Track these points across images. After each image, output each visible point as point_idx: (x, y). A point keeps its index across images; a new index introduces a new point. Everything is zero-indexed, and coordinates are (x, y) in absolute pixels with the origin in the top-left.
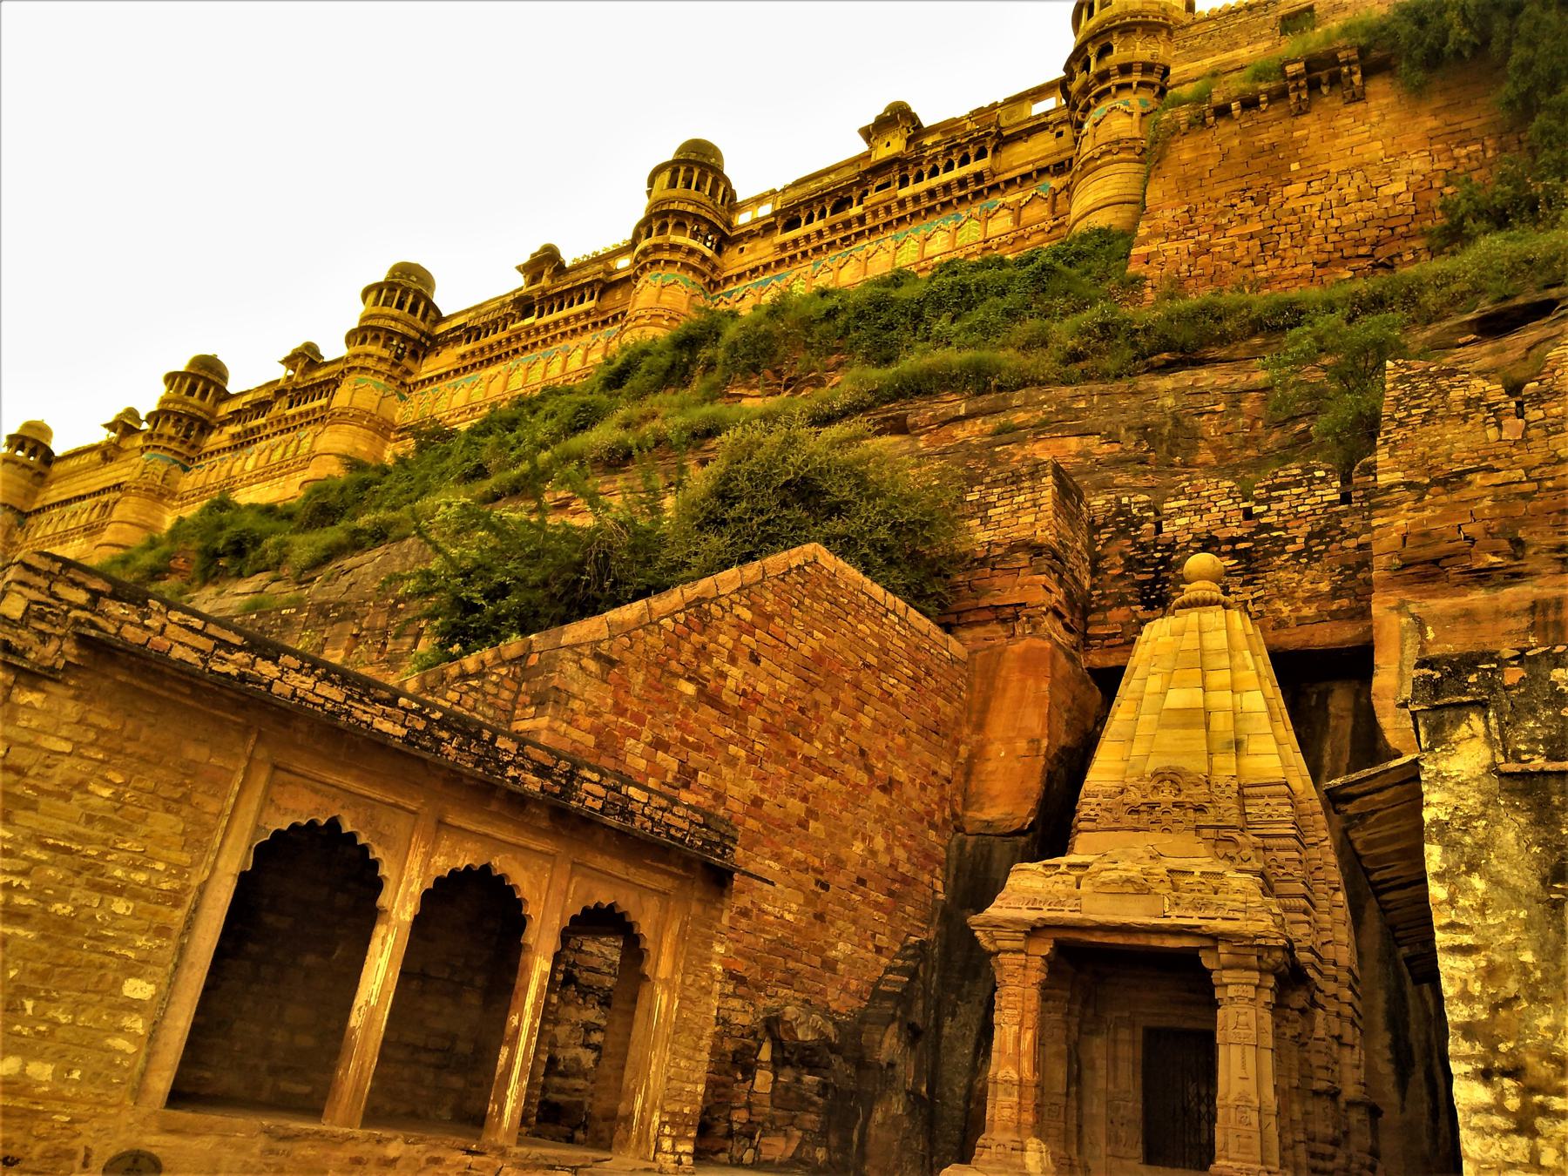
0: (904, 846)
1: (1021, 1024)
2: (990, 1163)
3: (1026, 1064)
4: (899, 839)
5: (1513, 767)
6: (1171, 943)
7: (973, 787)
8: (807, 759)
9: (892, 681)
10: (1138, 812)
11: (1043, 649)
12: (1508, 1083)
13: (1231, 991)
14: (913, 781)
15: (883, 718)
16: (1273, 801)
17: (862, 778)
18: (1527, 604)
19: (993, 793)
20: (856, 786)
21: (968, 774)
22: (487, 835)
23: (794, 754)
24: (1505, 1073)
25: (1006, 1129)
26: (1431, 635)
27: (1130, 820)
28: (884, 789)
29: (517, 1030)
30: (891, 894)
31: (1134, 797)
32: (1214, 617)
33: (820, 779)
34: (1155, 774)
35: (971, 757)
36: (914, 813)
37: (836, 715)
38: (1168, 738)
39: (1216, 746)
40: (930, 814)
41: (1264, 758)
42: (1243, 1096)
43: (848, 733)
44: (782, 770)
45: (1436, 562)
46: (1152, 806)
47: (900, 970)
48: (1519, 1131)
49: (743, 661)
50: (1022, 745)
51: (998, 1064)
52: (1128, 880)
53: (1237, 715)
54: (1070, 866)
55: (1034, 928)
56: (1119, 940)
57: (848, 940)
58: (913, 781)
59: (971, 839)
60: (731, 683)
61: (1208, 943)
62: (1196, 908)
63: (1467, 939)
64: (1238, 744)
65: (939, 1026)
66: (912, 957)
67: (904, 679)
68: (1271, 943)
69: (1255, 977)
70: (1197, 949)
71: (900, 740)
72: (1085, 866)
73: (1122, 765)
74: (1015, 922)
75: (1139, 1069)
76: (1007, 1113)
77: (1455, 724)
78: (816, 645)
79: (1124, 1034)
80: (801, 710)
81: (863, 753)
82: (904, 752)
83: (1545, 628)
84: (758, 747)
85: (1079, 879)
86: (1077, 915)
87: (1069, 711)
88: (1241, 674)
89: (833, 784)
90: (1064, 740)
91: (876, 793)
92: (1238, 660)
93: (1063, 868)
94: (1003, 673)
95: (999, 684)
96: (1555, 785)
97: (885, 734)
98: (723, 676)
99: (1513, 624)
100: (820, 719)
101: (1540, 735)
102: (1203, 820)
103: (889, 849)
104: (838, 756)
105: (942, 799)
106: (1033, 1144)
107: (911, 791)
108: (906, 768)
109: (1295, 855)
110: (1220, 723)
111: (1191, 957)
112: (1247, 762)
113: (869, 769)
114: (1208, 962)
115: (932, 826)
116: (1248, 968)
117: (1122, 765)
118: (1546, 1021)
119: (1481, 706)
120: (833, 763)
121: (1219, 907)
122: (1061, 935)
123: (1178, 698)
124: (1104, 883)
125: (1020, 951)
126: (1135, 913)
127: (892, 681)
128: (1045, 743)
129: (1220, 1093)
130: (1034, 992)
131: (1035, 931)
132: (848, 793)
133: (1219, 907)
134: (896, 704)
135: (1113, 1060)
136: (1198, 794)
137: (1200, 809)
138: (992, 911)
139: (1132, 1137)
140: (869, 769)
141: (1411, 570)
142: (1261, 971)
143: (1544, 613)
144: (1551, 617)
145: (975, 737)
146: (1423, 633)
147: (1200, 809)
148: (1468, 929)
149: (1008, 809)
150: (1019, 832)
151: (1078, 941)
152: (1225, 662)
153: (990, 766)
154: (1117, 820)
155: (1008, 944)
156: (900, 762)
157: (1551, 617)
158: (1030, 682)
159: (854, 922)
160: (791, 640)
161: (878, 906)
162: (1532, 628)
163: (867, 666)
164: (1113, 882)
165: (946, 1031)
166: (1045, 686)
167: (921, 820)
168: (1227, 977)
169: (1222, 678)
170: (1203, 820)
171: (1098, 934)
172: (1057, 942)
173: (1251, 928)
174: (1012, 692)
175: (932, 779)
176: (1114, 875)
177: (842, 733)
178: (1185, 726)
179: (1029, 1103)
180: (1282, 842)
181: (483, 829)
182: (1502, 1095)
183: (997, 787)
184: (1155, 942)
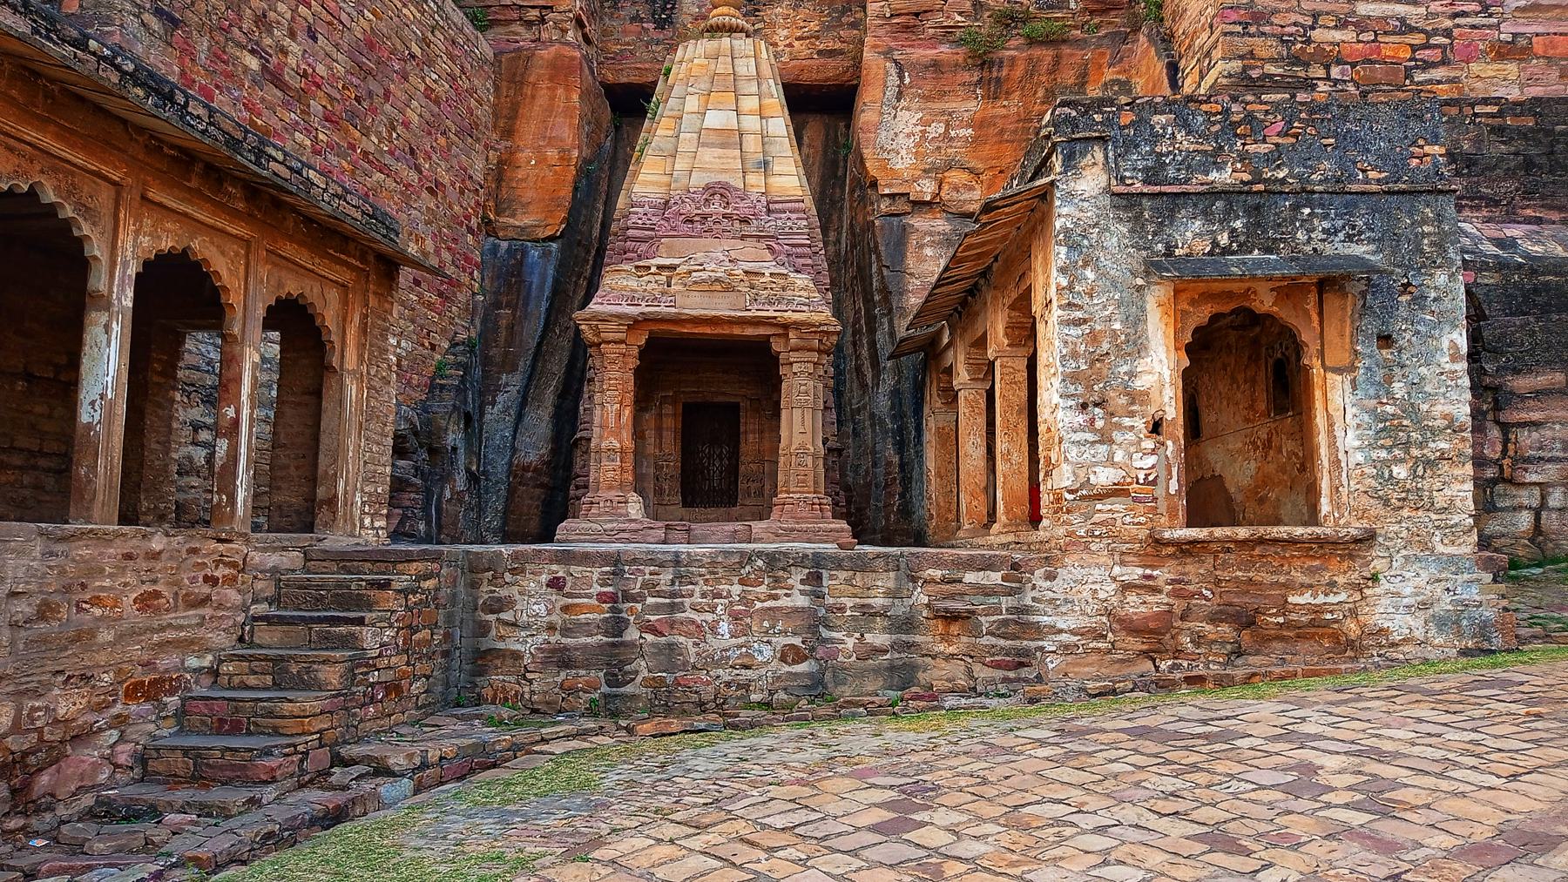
0: (449, 249)
1: (621, 403)
3: (626, 435)
4: (445, 242)
5: (1121, 189)
6: (750, 331)
7: (504, 193)
8: (365, 153)
9: (435, 76)
10: (692, 222)
11: (573, 58)
12: (1097, 410)
13: (796, 368)
14: (453, 184)
15: (427, 115)
16: (794, 216)
17: (413, 177)
19: (524, 200)
20: (408, 186)
21: (499, 180)
22: (186, 215)
23: (353, 147)
24: (1096, 405)
25: (610, 488)
26: (907, 81)
27: (686, 227)
28: (431, 191)
29: (236, 422)
30: (440, 294)
31: (689, 208)
32: (742, 44)
33: (378, 176)
34: (707, 188)
35: (500, 162)
36: (455, 217)
37: (387, 107)
38: (708, 156)
39: (749, 166)
40: (468, 218)
41: (784, 179)
42: (802, 446)
43: (400, 129)
44: (344, 164)
45: (917, 15)
46: (705, 217)
47: (458, 365)
48: (1101, 442)
49: (302, 36)
50: (552, 153)
51: (601, 437)
52: (717, 280)
53: (764, 137)
54: (659, 267)
55: (636, 321)
57: (408, 338)
58: (453, 184)
59: (504, 245)
60: (292, 61)
62: (770, 303)
63: (1079, 314)
64: (766, 163)
65: (482, 414)
66: (463, 353)
67: (444, 76)
68: (832, 329)
69: (815, 356)
71: (442, 141)
72: (673, 268)
73: (666, 179)
74: (619, 316)
75: (679, 437)
76: (610, 474)
77: (1083, 154)
78: (366, 25)
79: (668, 409)
80: (357, 99)
81: (412, 152)
82: (446, 153)
84: (321, 136)
85: (669, 278)
86: (673, 310)
87: (589, 123)
88: (766, 101)
89: (391, 184)
90: (586, 152)
91: (425, 194)
92: (764, 86)
93: (653, 270)
94: (531, 79)
95: (528, 91)
96: (1146, 203)
97: (430, 133)
98: (284, 51)
100: (374, 111)
101: (1140, 165)
102: (747, 230)
103: (437, 252)
104: (391, 153)
105: (477, 203)
106: (634, 497)
107: (453, 195)
108: (447, 171)
109: (809, 261)
110: (752, 144)
111: (764, 343)
112: (772, 180)
113: (418, 169)
114: (777, 346)
115: (470, 230)
116: (811, 350)
117: (666, 179)
118: (1125, 368)
119: (1102, 140)
120: (388, 160)
121: (790, 302)
122: (655, 327)
123: (714, 119)
125: (622, 342)
126: (721, 307)
127: (435, 76)
128: (576, 153)
129: (782, 445)
130: (630, 376)
131: (636, 323)
132: (402, 193)
133: (790, 302)
134: (437, 102)
135: (659, 430)
136: (743, 208)
137: (745, 221)
138: (593, 307)
139: (672, 487)
140: (418, 169)
142: (820, 351)
143: (990, 68)
144: (995, 74)
145: (504, 143)
146: (901, 78)
147: (745, 221)
148: (1080, 308)
149: (540, 216)
150: (552, 238)
151: (670, 332)
152: (754, 89)
153: (520, 174)
155: (611, 336)
156: (442, 163)
157: (995, 74)
158: (560, 91)
159: (413, 322)
160: (344, 17)
161: (430, 306)
162: (980, 81)
163: (413, 57)
164: (704, 281)
165: (488, 417)
166: (575, 97)
167: (461, 224)
168: (794, 356)
169: (750, 103)
170: (747, 230)
173: (816, 318)
174: (542, 99)
175: (468, 182)
176: (704, 275)
177: (394, 129)
178: (724, 146)
179: (629, 466)
180: (799, 250)
181: (182, 208)
182: (1092, 421)
183: (529, 195)
184: (737, 331)
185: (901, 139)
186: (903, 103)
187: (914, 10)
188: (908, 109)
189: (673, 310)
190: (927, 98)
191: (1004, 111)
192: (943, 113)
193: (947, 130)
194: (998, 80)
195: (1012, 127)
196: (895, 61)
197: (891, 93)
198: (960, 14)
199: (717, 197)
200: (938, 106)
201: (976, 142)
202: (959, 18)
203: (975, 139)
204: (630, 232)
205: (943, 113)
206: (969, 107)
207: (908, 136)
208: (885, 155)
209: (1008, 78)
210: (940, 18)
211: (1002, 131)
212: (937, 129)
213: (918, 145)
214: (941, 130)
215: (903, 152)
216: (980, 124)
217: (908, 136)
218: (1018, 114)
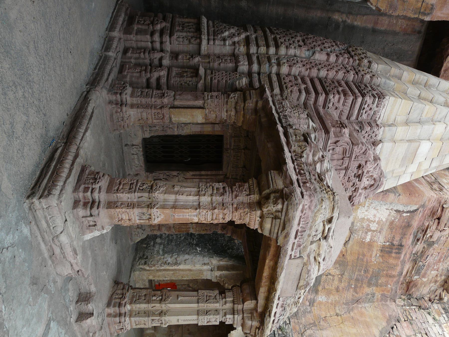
2: (77, 218)
18: (403, 244)
25: (111, 217)
26: (405, 215)
31: (370, 167)
45: (439, 219)
56: (266, 273)
61: (260, 310)
70: (256, 299)
74: (287, 236)
76: (125, 217)
83: (391, 248)
99: (397, 238)
114: (249, 304)
124: (309, 271)
141: (439, 211)
144: (394, 251)
154: (356, 157)
171: (272, 263)
172: (269, 239)
185: (373, 212)
186: (393, 213)
187: (442, 219)
188: (389, 215)
189: (288, 257)
190: (392, 223)
191: (374, 255)
192: (382, 229)
193: (370, 230)
194: (391, 252)
195: (365, 260)
196: (416, 210)
197: (401, 208)
198: (431, 237)
199: (372, 182)
200: (386, 227)
201: (362, 243)
202: (429, 235)
203: (363, 243)
204: (360, 100)
205: (382, 229)
206: (381, 240)
207: (375, 216)
208: (367, 205)
209: (390, 256)
210: (434, 227)
211: (364, 255)
212: (374, 226)
213: (368, 220)
214: (373, 229)
215: (366, 213)
216: (370, 245)
217: (375, 216)
218: (371, 261)
